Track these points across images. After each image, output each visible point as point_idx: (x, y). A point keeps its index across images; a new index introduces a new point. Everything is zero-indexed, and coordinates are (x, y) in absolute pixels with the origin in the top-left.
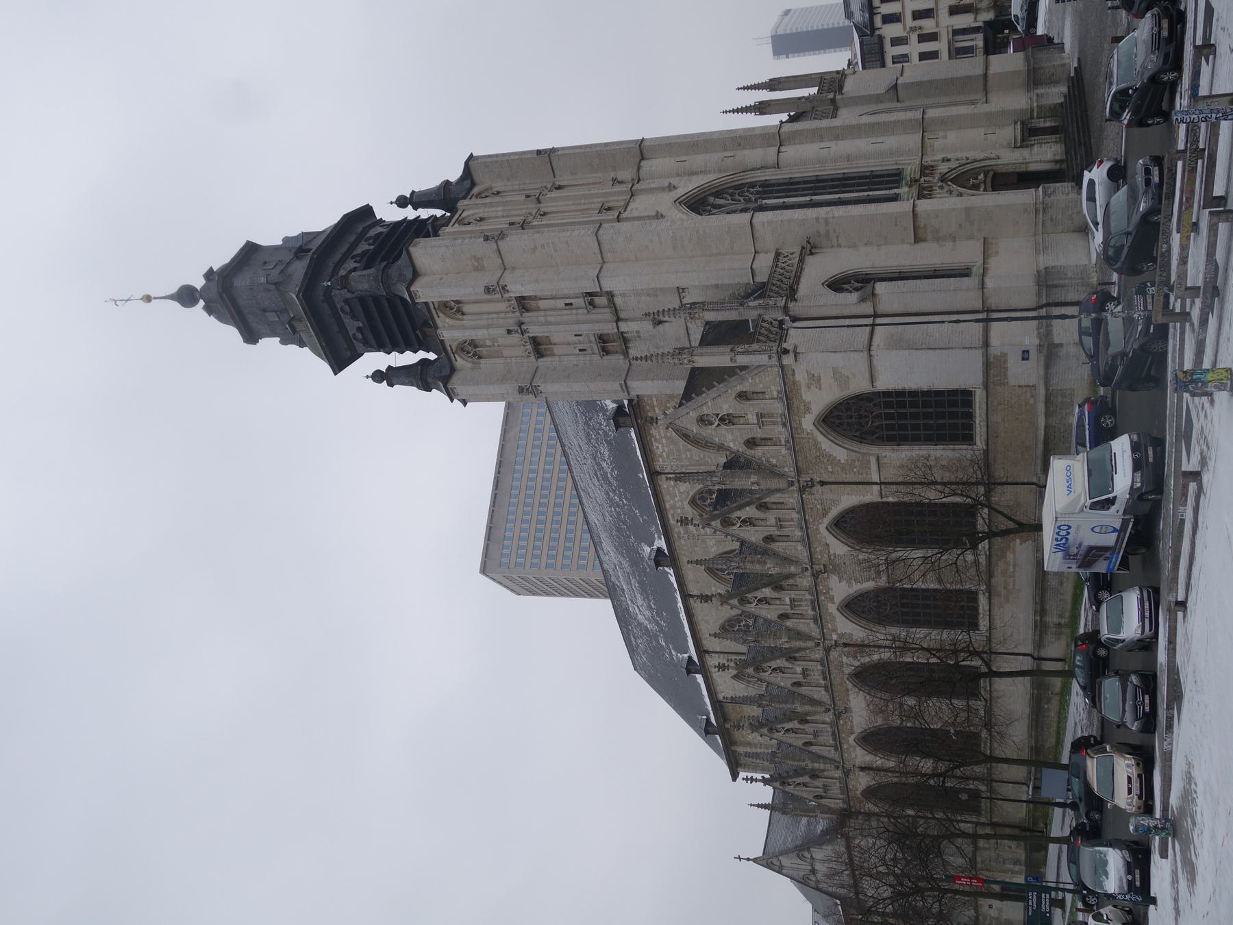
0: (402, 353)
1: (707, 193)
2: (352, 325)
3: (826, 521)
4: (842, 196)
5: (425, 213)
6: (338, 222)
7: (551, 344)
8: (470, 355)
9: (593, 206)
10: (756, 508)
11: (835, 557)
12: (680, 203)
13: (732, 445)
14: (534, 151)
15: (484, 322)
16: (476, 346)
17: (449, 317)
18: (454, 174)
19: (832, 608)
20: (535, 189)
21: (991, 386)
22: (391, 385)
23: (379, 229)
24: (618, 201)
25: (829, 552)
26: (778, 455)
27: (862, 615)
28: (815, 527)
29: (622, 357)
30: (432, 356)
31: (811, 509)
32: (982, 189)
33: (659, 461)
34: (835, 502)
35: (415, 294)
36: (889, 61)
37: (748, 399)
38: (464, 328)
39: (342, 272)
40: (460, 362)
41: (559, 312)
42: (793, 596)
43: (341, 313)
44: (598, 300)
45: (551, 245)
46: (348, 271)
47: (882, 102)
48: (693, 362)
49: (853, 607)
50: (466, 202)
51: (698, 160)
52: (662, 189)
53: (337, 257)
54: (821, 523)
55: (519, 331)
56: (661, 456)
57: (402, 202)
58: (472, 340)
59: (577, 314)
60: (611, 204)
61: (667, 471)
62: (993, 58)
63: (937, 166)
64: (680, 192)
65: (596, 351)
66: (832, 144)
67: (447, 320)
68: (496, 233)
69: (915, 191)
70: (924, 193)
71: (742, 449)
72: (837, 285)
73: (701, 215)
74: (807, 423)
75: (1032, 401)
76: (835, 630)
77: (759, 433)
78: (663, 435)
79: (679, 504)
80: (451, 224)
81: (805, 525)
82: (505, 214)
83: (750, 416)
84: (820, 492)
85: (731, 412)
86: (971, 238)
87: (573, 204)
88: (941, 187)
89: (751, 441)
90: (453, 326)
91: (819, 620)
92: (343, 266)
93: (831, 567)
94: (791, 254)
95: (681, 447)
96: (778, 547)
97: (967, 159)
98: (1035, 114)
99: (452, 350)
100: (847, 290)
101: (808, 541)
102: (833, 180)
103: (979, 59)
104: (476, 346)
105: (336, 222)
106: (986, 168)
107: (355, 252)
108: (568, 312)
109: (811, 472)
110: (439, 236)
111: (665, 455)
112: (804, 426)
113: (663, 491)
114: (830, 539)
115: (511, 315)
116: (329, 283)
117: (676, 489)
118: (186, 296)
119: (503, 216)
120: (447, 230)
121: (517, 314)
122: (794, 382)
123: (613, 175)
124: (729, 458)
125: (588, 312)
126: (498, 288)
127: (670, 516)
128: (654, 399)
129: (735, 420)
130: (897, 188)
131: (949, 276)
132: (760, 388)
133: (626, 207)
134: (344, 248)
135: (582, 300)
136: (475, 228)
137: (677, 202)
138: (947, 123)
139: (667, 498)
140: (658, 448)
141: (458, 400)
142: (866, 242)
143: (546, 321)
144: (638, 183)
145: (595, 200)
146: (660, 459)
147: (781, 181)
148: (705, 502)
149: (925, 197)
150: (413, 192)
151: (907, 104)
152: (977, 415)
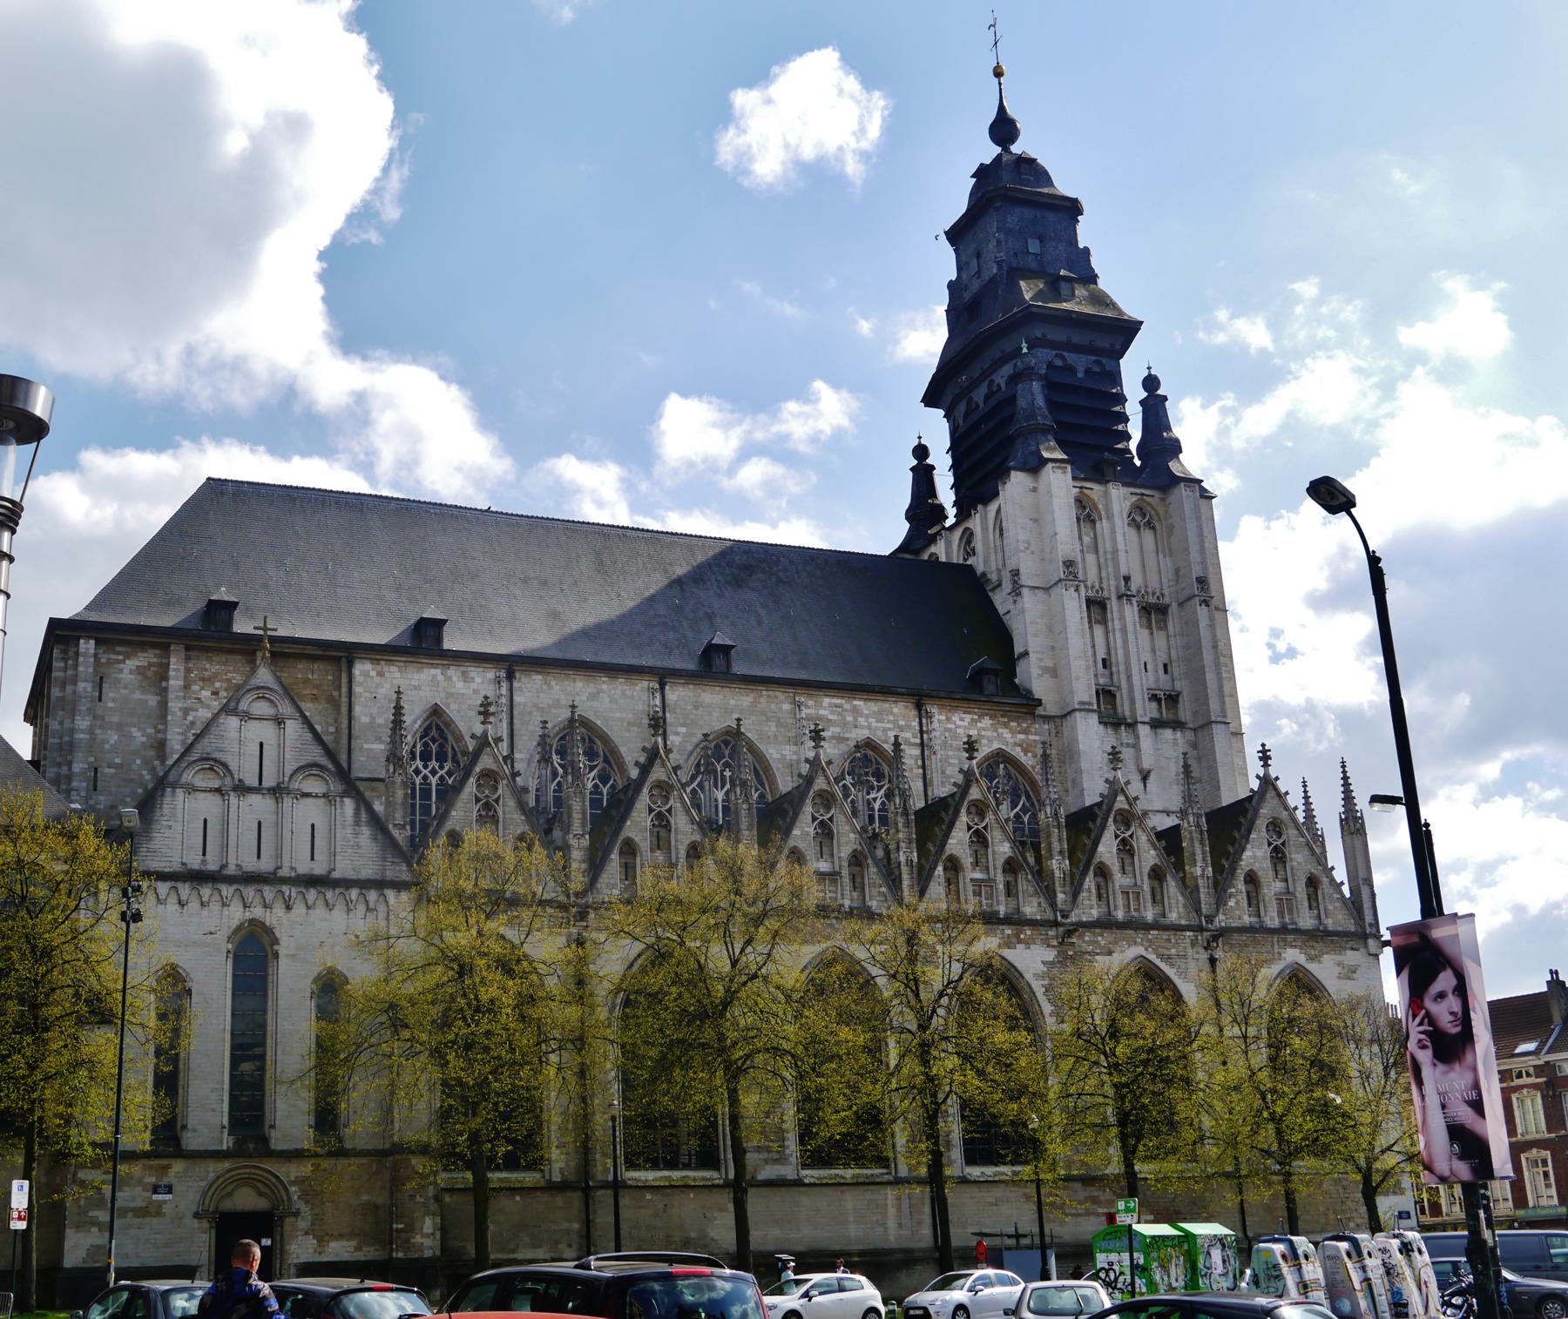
31: (1169, 940)
33: (940, 714)
34: (1184, 974)
56: (948, 719)
79: (862, 721)
93: (1070, 953)
96: (1090, 882)
109: (1227, 948)
111: (949, 726)
113: (886, 705)
117: (891, 726)
127: (838, 701)
140: (962, 719)
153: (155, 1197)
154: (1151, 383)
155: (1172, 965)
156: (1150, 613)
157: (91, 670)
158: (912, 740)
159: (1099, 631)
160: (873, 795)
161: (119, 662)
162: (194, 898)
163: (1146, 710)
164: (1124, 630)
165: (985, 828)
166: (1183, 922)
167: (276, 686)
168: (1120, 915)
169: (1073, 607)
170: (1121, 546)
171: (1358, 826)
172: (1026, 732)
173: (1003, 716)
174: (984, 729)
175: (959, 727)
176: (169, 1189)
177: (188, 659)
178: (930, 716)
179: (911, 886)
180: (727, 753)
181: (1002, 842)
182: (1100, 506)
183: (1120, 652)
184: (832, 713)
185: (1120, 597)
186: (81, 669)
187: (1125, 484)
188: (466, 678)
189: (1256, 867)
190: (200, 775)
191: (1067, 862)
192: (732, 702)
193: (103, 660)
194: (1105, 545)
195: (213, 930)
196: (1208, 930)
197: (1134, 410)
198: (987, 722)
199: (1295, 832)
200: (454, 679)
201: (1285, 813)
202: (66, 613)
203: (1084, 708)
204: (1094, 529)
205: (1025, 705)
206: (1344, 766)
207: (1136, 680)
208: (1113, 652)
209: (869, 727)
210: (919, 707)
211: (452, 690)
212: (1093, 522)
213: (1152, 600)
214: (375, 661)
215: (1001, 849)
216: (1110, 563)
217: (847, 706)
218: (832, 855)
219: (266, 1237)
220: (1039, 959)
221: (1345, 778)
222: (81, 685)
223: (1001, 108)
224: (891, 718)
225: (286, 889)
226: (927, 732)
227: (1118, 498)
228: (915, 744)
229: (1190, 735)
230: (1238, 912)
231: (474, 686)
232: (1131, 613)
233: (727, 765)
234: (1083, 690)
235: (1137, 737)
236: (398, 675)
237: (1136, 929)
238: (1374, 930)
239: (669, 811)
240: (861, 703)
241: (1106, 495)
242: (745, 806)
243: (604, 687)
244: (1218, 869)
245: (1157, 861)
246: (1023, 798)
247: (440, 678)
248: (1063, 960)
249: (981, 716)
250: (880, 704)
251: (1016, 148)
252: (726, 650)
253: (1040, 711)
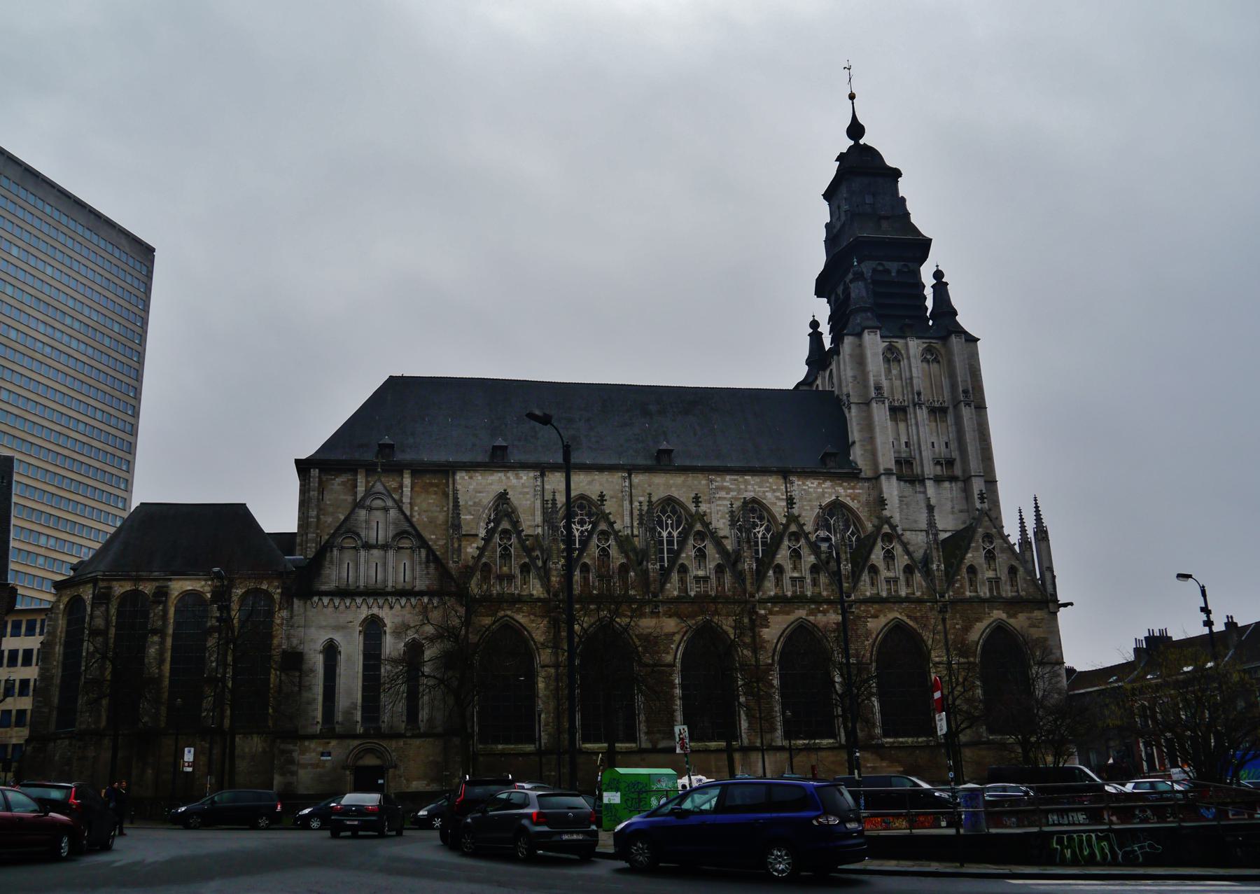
10: (908, 564)
11: (864, 622)
28: (896, 609)
33: (798, 481)
56: (804, 484)
76: (771, 613)
78: (826, 490)
96: (865, 577)
111: (804, 487)
113: (765, 478)
114: (883, 620)
127: (738, 477)
139: (757, 479)
140: (812, 483)
146: (800, 483)
153: (322, 758)
154: (938, 275)
156: (936, 414)
157: (317, 485)
158: (781, 497)
159: (902, 426)
160: (757, 530)
161: (332, 479)
162: (342, 604)
163: (929, 469)
164: (917, 424)
165: (800, 547)
166: (925, 597)
167: (384, 492)
168: (884, 594)
169: (880, 413)
170: (915, 375)
171: (1044, 535)
172: (853, 488)
173: (839, 480)
174: (826, 488)
175: (809, 488)
176: (329, 754)
177: (367, 476)
178: (792, 483)
179: (752, 584)
180: (669, 510)
181: (810, 555)
182: (903, 352)
183: (915, 437)
184: (731, 484)
185: (915, 405)
186: (312, 484)
187: (918, 338)
188: (518, 478)
189: (975, 563)
190: (346, 541)
191: (850, 565)
192: (671, 482)
193: (324, 479)
194: (906, 374)
195: (352, 620)
196: (940, 602)
197: (929, 292)
198: (828, 484)
199: (1001, 541)
200: (511, 478)
201: (994, 530)
202: (304, 456)
203: (888, 473)
204: (900, 365)
205: (852, 475)
206: (1036, 500)
207: (924, 454)
208: (911, 437)
209: (754, 491)
210: (785, 478)
211: (510, 484)
212: (899, 361)
213: (937, 405)
214: (467, 471)
215: (809, 560)
216: (909, 385)
217: (740, 480)
218: (706, 567)
219: (381, 779)
221: (1037, 507)
222: (312, 493)
223: (854, 117)
224: (768, 485)
225: (390, 598)
226: (790, 492)
227: (915, 346)
228: (783, 499)
229: (960, 484)
231: (523, 481)
232: (922, 414)
233: (669, 517)
234: (886, 460)
235: (925, 488)
236: (480, 478)
237: (894, 603)
238: (1053, 598)
239: (609, 546)
240: (750, 477)
241: (907, 344)
242: (652, 542)
243: (596, 477)
244: (948, 565)
245: (909, 562)
246: (852, 527)
247: (504, 478)
249: (825, 481)
250: (761, 477)
251: (862, 142)
252: (669, 452)
253: (863, 475)
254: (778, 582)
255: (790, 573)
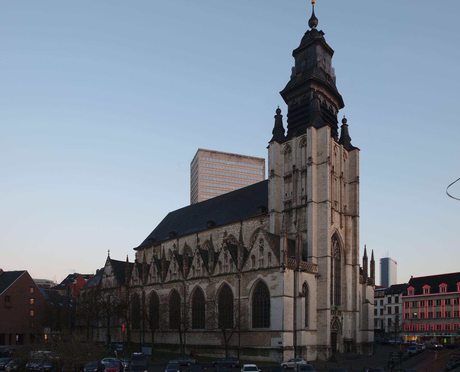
0: (287, 121)
1: (338, 240)
2: (298, 100)
3: (227, 282)
4: (334, 286)
5: (339, 130)
6: (339, 93)
7: (289, 183)
8: (286, 150)
9: (337, 199)
10: (231, 259)
12: (336, 231)
13: (253, 250)
14: (359, 176)
15: (298, 156)
16: (289, 153)
17: (300, 142)
18: (353, 143)
19: (197, 283)
20: (345, 176)
21: (271, 333)
22: (275, 117)
23: (335, 111)
24: (338, 208)
25: (216, 283)
26: (249, 265)
27: (195, 293)
28: (224, 278)
29: (283, 210)
30: (286, 134)
31: (231, 277)
32: (332, 330)
34: (233, 285)
35: (310, 128)
36: (376, 299)
37: (268, 256)
38: (296, 148)
39: (319, 96)
40: (283, 146)
41: (300, 186)
42: (201, 271)
43: (303, 95)
44: (304, 201)
45: (325, 183)
46: (320, 99)
47: (363, 298)
48: (282, 237)
49: (198, 290)
50: (342, 148)
51: (350, 238)
52: (341, 224)
53: (325, 93)
54: (226, 280)
55: (294, 170)
57: (344, 121)
58: (291, 151)
59: (299, 193)
60: (337, 205)
61: (242, 226)
62: (373, 332)
63: (341, 316)
64: (340, 231)
65: (286, 200)
66: (351, 282)
67: (299, 141)
68: (330, 162)
69: (334, 309)
70: (333, 312)
71: (251, 254)
72: (305, 285)
73: (331, 238)
74: (260, 276)
75: (266, 345)
77: (257, 260)
80: (335, 142)
81: (225, 274)
82: (337, 164)
83: (262, 257)
84: (236, 280)
85: (264, 250)
86: (317, 326)
87: (338, 191)
88: (334, 317)
89: (254, 257)
90: (297, 143)
91: (193, 279)
92: (322, 96)
93: (211, 283)
94: (316, 270)
95: (251, 232)
96: (218, 266)
97: (342, 325)
98: (354, 345)
99: (288, 143)
100: (303, 288)
101: (220, 275)
102: (339, 283)
103: (373, 328)
104: (289, 153)
105: (339, 92)
106: (338, 331)
107: (327, 101)
108: (300, 189)
109: (243, 277)
110: (331, 138)
112: (259, 275)
114: (220, 283)
115: (300, 167)
116: (316, 91)
118: (313, 21)
119: (336, 164)
120: (333, 141)
121: (300, 170)
122: (274, 272)
123: (348, 206)
124: (247, 248)
125: (300, 197)
126: (310, 162)
128: (268, 222)
129: (261, 252)
130: (335, 304)
131: (306, 320)
132: (272, 260)
133: (336, 211)
134: (329, 96)
135: (304, 195)
136: (333, 152)
137: (336, 230)
138: (354, 319)
141: (269, 145)
142: (318, 294)
143: (298, 181)
144: (344, 215)
145: (339, 199)
147: (340, 266)
148: (231, 240)
149: (331, 312)
150: (348, 126)
151: (361, 306)
152: (261, 329)
155: (231, 283)
220: (205, 286)
230: (248, 267)
248: (210, 285)
254: (254, 262)
255: (258, 258)
